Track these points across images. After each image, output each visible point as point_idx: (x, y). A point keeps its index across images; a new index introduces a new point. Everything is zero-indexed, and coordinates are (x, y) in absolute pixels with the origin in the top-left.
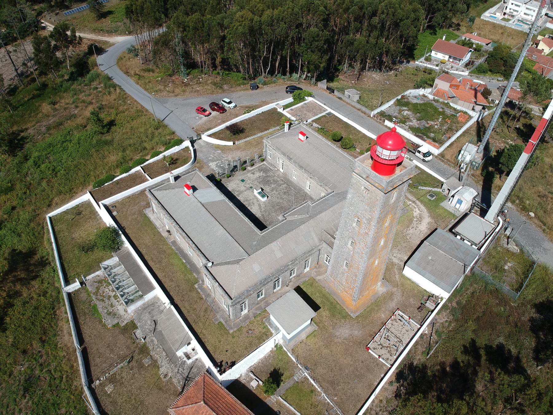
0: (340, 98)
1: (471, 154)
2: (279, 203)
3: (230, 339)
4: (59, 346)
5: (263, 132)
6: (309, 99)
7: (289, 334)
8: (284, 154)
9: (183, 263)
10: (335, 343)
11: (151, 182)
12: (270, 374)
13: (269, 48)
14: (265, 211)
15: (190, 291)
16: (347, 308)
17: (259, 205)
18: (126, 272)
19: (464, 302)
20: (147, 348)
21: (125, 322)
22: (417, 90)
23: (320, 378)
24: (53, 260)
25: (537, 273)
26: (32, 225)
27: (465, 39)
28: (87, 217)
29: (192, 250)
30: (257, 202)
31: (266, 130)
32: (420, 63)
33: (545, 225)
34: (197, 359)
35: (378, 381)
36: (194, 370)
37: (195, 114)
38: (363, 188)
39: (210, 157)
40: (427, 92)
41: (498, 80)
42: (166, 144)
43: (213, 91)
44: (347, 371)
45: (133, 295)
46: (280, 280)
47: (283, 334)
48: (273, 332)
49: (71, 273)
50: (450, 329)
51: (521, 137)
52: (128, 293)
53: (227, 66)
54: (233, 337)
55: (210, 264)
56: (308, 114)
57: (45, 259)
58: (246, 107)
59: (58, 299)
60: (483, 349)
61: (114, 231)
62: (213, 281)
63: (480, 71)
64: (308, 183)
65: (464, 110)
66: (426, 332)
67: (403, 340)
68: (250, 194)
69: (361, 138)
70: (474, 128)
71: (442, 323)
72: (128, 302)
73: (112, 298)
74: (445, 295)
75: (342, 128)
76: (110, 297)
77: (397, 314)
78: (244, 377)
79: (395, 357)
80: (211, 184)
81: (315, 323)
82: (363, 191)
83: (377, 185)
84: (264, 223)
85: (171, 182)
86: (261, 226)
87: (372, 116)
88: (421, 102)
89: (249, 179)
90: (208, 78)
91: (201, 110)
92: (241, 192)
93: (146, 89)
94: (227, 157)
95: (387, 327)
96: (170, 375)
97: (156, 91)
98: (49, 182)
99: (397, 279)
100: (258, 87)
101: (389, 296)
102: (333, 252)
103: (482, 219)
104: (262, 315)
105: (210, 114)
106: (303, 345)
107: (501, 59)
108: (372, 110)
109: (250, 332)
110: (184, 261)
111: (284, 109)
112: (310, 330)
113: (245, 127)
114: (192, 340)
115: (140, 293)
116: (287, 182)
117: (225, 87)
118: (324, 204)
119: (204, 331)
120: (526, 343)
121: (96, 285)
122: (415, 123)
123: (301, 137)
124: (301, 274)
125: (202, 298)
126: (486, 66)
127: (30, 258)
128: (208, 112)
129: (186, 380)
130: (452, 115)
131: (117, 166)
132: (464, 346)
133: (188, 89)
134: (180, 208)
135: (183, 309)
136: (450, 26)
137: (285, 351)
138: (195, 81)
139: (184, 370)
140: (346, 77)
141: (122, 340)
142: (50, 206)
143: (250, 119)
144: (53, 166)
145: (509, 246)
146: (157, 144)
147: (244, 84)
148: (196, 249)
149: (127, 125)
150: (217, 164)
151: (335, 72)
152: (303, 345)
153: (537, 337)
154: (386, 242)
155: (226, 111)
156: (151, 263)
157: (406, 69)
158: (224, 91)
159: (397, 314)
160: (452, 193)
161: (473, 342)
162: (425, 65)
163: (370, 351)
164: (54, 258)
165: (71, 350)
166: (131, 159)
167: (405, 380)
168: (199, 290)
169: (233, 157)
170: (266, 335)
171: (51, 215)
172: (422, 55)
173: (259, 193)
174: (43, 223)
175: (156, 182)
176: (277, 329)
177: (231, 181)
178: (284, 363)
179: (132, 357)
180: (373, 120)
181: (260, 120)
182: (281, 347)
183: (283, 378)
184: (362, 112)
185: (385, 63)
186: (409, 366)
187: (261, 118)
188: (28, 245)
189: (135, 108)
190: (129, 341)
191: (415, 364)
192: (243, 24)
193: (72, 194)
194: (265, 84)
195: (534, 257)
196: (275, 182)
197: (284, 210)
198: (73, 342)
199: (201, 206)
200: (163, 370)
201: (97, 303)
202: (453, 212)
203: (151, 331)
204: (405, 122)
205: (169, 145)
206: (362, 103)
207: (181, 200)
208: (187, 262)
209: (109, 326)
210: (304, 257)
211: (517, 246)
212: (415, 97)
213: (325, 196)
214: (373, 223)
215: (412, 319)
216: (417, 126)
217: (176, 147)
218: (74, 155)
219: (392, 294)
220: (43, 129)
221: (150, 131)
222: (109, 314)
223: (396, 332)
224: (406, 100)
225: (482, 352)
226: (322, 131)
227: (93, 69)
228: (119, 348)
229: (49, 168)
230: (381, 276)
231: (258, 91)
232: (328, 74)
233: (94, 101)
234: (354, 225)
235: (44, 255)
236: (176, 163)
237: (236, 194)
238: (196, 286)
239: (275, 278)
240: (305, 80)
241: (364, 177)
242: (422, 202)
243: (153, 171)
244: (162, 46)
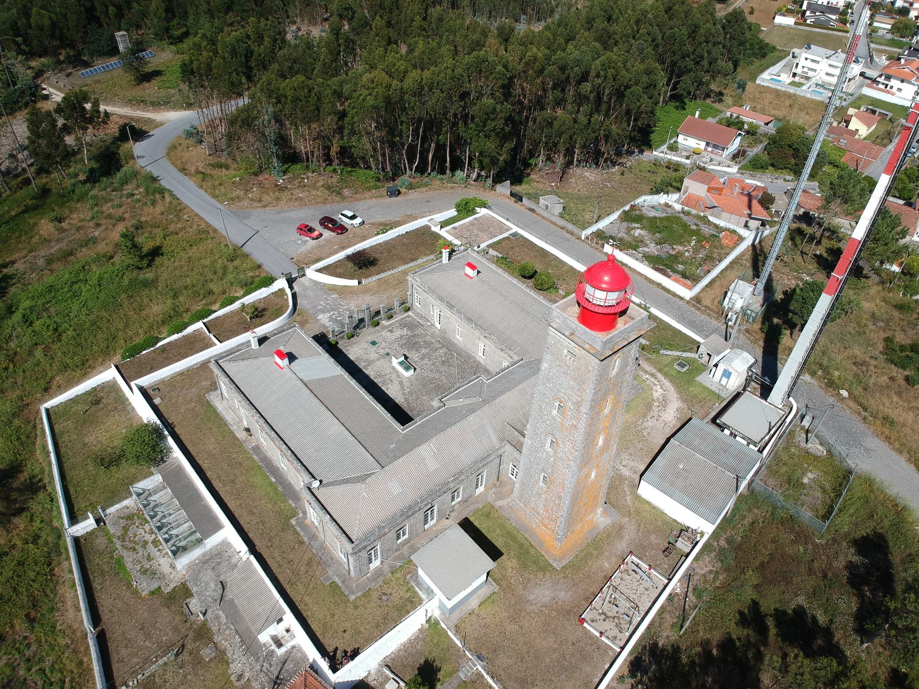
0: (532, 210)
1: (744, 296)
3: (350, 610)
4: (59, 628)
5: (407, 263)
7: (450, 600)
8: (441, 299)
9: (271, 483)
10: (528, 613)
11: (219, 348)
12: (419, 669)
13: (416, 131)
15: (283, 530)
17: (401, 383)
18: (175, 500)
19: (739, 539)
20: (209, 630)
21: (172, 586)
23: (502, 673)
24: (50, 482)
25: (856, 489)
26: (16, 422)
27: (731, 115)
28: (110, 407)
29: (286, 461)
30: (397, 378)
31: (413, 260)
32: (660, 153)
33: (866, 410)
34: (294, 647)
35: (600, 675)
36: (289, 666)
37: (295, 236)
38: (565, 351)
39: (319, 305)
40: (672, 199)
41: (785, 180)
42: (246, 285)
43: (326, 199)
44: (547, 660)
45: (185, 538)
46: (435, 508)
47: (440, 601)
48: (423, 596)
49: (79, 504)
50: (717, 584)
51: (825, 270)
52: (177, 536)
53: (349, 158)
54: (356, 608)
55: (316, 484)
56: (481, 234)
57: (36, 480)
58: (381, 224)
59: (57, 548)
60: (771, 616)
61: (156, 431)
62: (322, 513)
63: (756, 166)
64: (481, 345)
65: (732, 227)
66: (678, 591)
67: (640, 605)
68: (385, 366)
70: (749, 256)
71: (704, 575)
72: (177, 552)
73: (150, 545)
74: (708, 528)
76: (146, 543)
77: (630, 562)
78: (373, 676)
79: (628, 634)
80: (320, 349)
81: (494, 580)
82: (566, 356)
84: (409, 413)
85: (253, 347)
86: (403, 417)
88: (663, 215)
89: (384, 340)
90: (318, 178)
91: (306, 230)
92: (370, 363)
93: (215, 197)
94: (348, 304)
95: (613, 583)
96: (247, 675)
97: (232, 199)
98: (47, 349)
99: (629, 502)
100: (399, 193)
101: (617, 531)
102: (523, 460)
103: (763, 401)
104: (404, 569)
105: (321, 235)
106: (474, 618)
107: (790, 146)
109: (385, 598)
110: (274, 480)
111: (441, 227)
113: (377, 256)
114: (285, 613)
115: (198, 535)
116: (448, 345)
117: (346, 192)
118: (508, 380)
119: (306, 598)
120: (842, 605)
121: (123, 522)
122: (652, 249)
123: (469, 271)
124: (470, 497)
125: (302, 543)
126: (765, 157)
127: (12, 477)
128: (316, 233)
129: (275, 683)
130: (713, 236)
131: (164, 322)
132: (741, 613)
133: (285, 195)
134: (267, 390)
135: (270, 562)
136: (708, 96)
137: (443, 629)
138: (296, 182)
139: (271, 665)
141: (165, 616)
142: (48, 391)
143: (386, 243)
144: (55, 322)
145: (809, 445)
146: (232, 284)
147: (377, 188)
148: (292, 458)
149: (182, 253)
150: (330, 317)
152: (474, 618)
153: (861, 595)
154: (607, 441)
155: (347, 230)
156: (216, 484)
158: (344, 198)
159: (630, 562)
160: (715, 359)
161: (755, 605)
162: (669, 157)
163: (585, 625)
164: (53, 478)
165: (79, 634)
166: (188, 310)
167: (645, 672)
168: (298, 529)
169: (357, 306)
170: (412, 602)
171: (49, 404)
172: (663, 142)
173: (401, 363)
174: (35, 419)
175: (229, 347)
176: (430, 593)
177: (354, 343)
179: (183, 646)
181: (404, 244)
182: (437, 623)
183: (440, 675)
186: (651, 648)
187: (405, 241)
188: (9, 457)
189: (195, 227)
190: (178, 618)
191: (660, 644)
192: (374, 93)
193: (85, 369)
194: (411, 187)
195: (851, 463)
196: (428, 344)
197: (441, 390)
198: (82, 622)
199: (303, 386)
200: (235, 667)
201: (125, 553)
202: (717, 391)
203: (216, 600)
204: (638, 247)
205: (250, 286)
207: (269, 378)
208: (278, 481)
209: (143, 594)
210: (476, 468)
211: (821, 444)
212: (653, 207)
213: (508, 367)
214: (584, 409)
215: (655, 569)
216: (657, 253)
217: (263, 289)
218: (90, 304)
219: (621, 528)
220: (41, 262)
221: (219, 265)
222: (144, 572)
223: (629, 591)
225: (770, 622)
227: (127, 163)
228: (160, 631)
229: (48, 326)
230: (602, 499)
231: (400, 198)
233: (127, 216)
234: (555, 412)
235: (36, 471)
236: (262, 316)
237: (361, 365)
238: (293, 522)
239: (426, 505)
241: (567, 334)
242: (666, 375)
243: (223, 330)
244: (241, 127)
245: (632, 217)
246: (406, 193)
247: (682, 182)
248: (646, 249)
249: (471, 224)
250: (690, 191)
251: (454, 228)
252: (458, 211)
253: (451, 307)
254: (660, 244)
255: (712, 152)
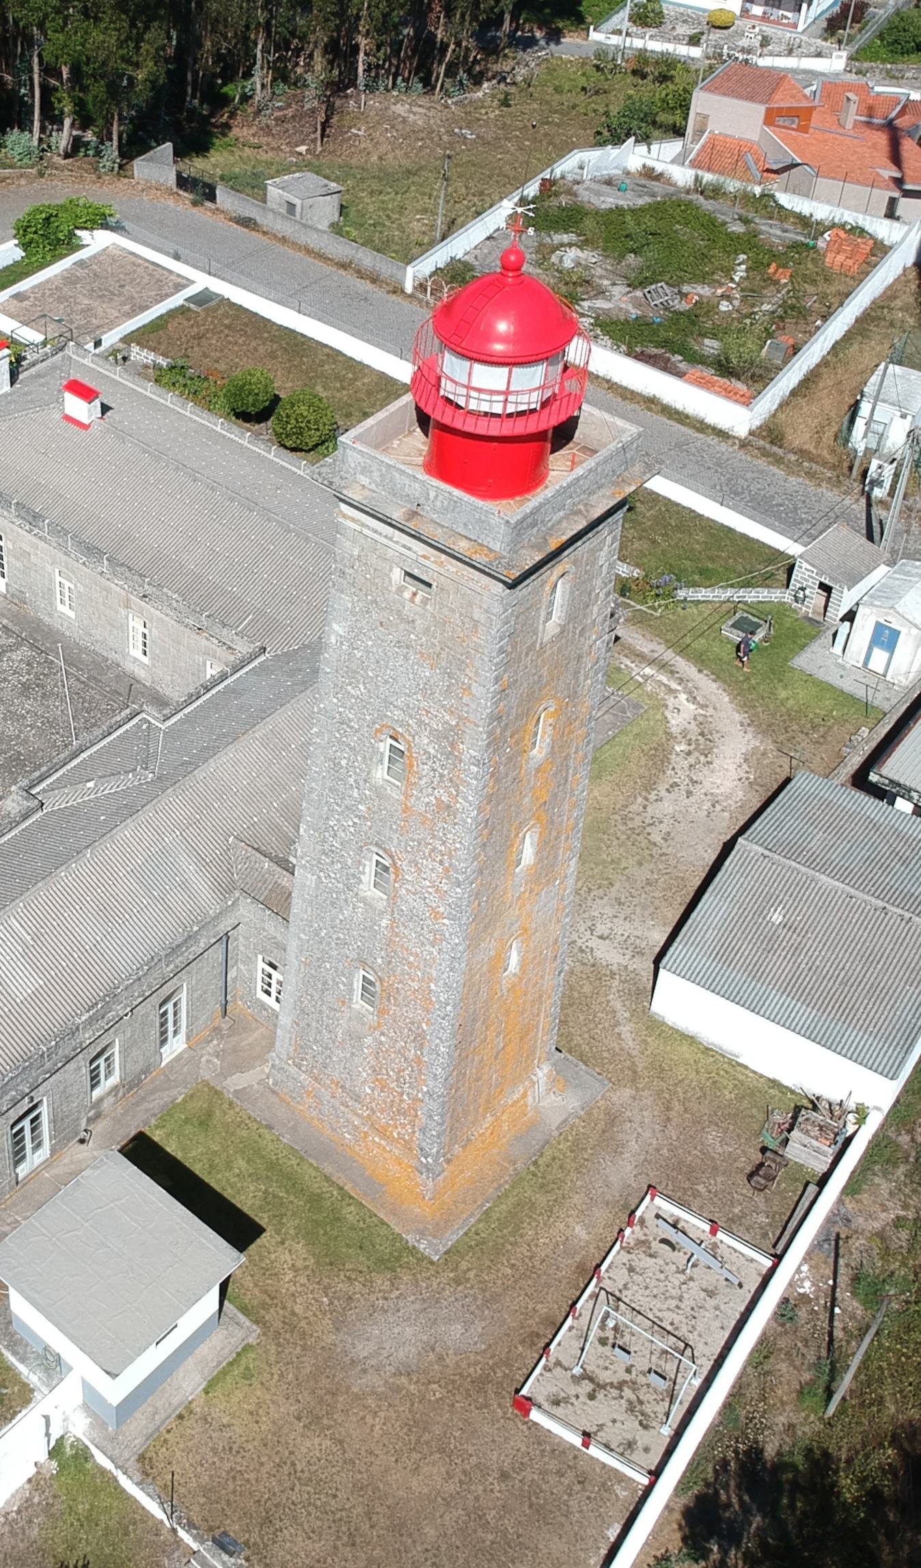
6: (96, 241)
7: (114, 1376)
16: (394, 1213)
22: (612, 152)
46: (44, 1110)
47: (85, 1385)
48: (33, 1378)
56: (100, 307)
64: (136, 624)
69: (369, 393)
75: (272, 355)
81: (244, 1310)
83: (462, 546)
87: (409, 288)
102: (295, 940)
106: (193, 1427)
108: (409, 259)
112: (223, 1344)
118: (222, 713)
122: (620, 300)
124: (146, 1071)
137: (103, 1472)
140: (267, 130)
151: (212, 115)
152: (193, 1427)
157: (551, 71)
176: (53, 1366)
178: (107, 1531)
180: (415, 307)
182: (82, 1455)
184: (361, 274)
185: (444, 48)
206: (354, 233)
210: (154, 980)
212: (609, 182)
213: (223, 677)
216: (634, 312)
224: (564, 200)
226: (175, 377)
232: (180, 116)
240: (67, 156)
245: (555, 213)
247: (685, 106)
248: (605, 305)
249: (69, 279)
250: (715, 127)
251: (18, 297)
252: (25, 246)
253: (34, 519)
254: (642, 284)
255: (765, 18)
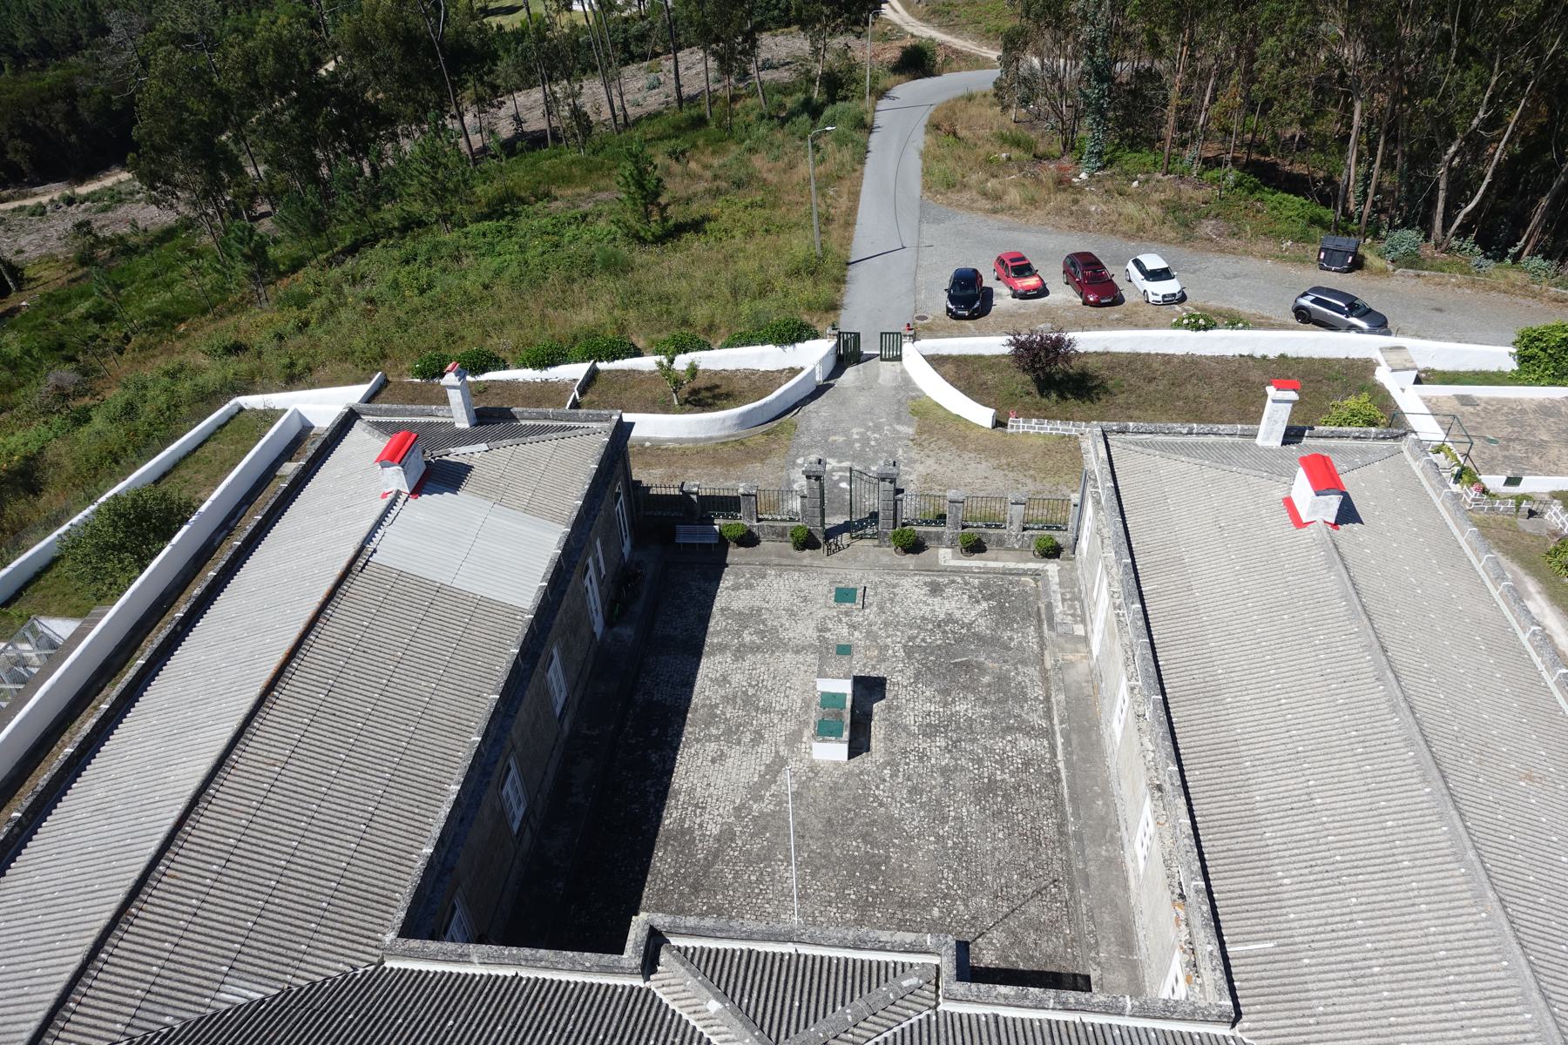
2: (891, 824)
14: (763, 824)
105: (1042, 292)
111: (1418, 381)
128: (1032, 282)
177: (800, 568)
217: (770, 348)
246: (1383, 272)
